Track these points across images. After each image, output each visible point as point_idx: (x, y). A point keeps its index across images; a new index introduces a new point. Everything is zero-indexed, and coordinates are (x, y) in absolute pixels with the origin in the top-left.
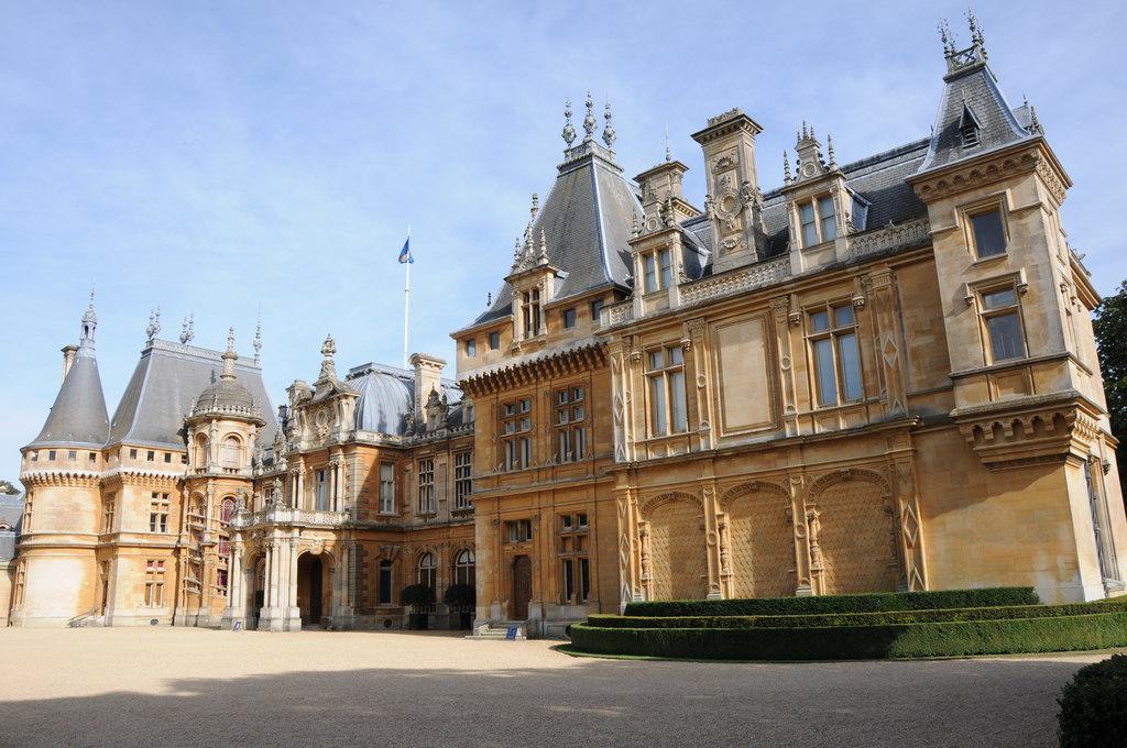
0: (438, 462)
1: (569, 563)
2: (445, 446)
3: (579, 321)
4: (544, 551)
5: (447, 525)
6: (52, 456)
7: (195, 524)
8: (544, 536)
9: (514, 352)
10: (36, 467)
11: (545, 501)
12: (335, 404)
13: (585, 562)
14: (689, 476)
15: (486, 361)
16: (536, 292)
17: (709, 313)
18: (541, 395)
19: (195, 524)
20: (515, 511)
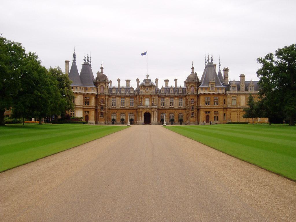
0: (165, 99)
1: (215, 117)
2: (168, 96)
3: (220, 90)
4: (212, 115)
5: (169, 109)
6: (76, 88)
7: (101, 104)
8: (212, 113)
9: (210, 91)
10: (77, 90)
11: (212, 110)
12: (152, 87)
13: (217, 117)
14: (237, 110)
15: (205, 92)
16: (213, 85)
17: (240, 94)
18: (212, 97)
19: (101, 104)
20: (207, 110)
